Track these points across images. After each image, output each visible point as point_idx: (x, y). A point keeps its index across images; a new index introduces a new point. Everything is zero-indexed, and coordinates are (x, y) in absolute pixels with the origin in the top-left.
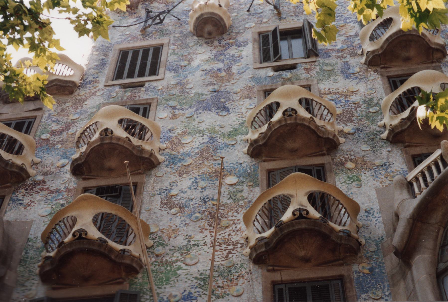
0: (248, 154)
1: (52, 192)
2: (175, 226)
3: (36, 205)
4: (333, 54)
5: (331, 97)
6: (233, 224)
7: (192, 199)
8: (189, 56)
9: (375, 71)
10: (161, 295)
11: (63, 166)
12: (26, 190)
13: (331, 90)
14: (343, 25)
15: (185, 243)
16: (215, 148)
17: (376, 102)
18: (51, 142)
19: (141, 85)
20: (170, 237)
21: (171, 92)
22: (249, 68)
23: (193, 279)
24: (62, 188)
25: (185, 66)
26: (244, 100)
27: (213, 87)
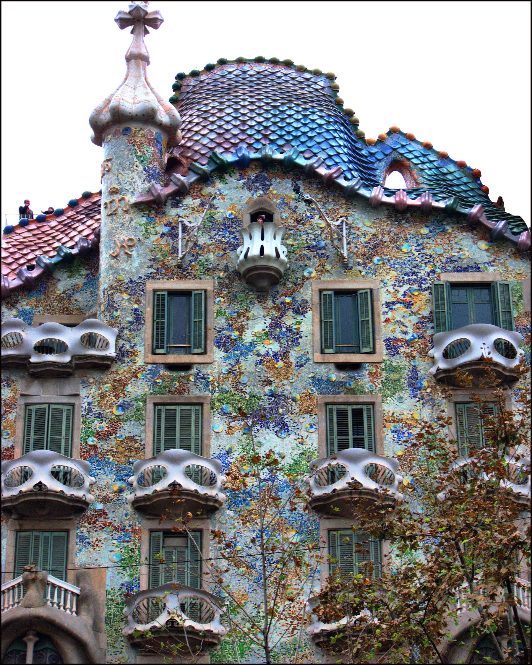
1: (116, 529)
2: (243, 590)
3: (104, 547)
4: (402, 349)
5: (395, 427)
8: (239, 321)
9: (444, 391)
11: (121, 491)
12: (90, 524)
13: (395, 415)
14: (416, 293)
15: (255, 613)
16: (277, 489)
18: (100, 451)
19: (187, 367)
21: (224, 386)
22: (308, 359)
24: (127, 523)
25: (236, 340)
26: (305, 416)
27: (270, 388)
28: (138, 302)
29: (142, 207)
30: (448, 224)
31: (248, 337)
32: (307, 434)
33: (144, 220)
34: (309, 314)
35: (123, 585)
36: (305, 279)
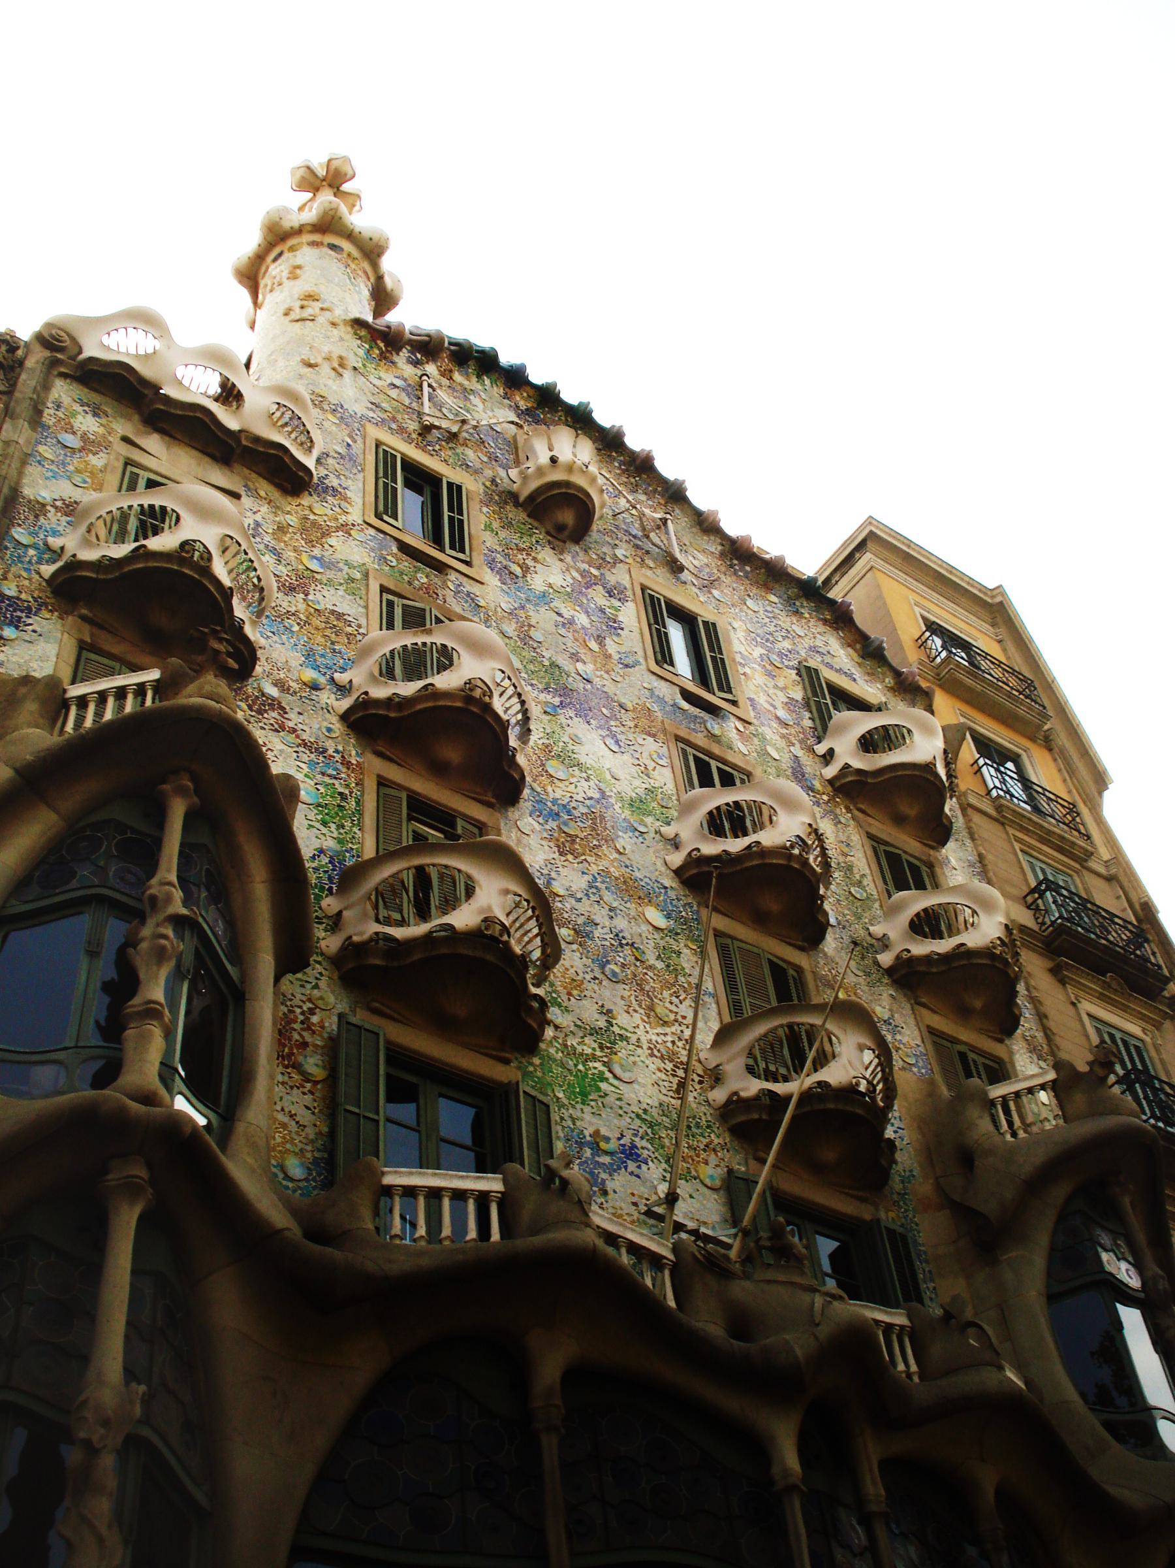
0: (678, 872)
1: (304, 744)
6: (676, 1021)
7: (597, 924)
8: (520, 557)
9: (848, 810)
10: (578, 1123)
11: (315, 687)
12: (250, 708)
15: (602, 1023)
17: (858, 877)
20: (569, 994)
23: (633, 1115)
24: (331, 747)
28: (351, 437)
29: (363, 333)
30: (802, 606)
31: (538, 582)
32: (654, 765)
33: (361, 352)
34: (630, 605)
35: (321, 851)
36: (617, 561)
